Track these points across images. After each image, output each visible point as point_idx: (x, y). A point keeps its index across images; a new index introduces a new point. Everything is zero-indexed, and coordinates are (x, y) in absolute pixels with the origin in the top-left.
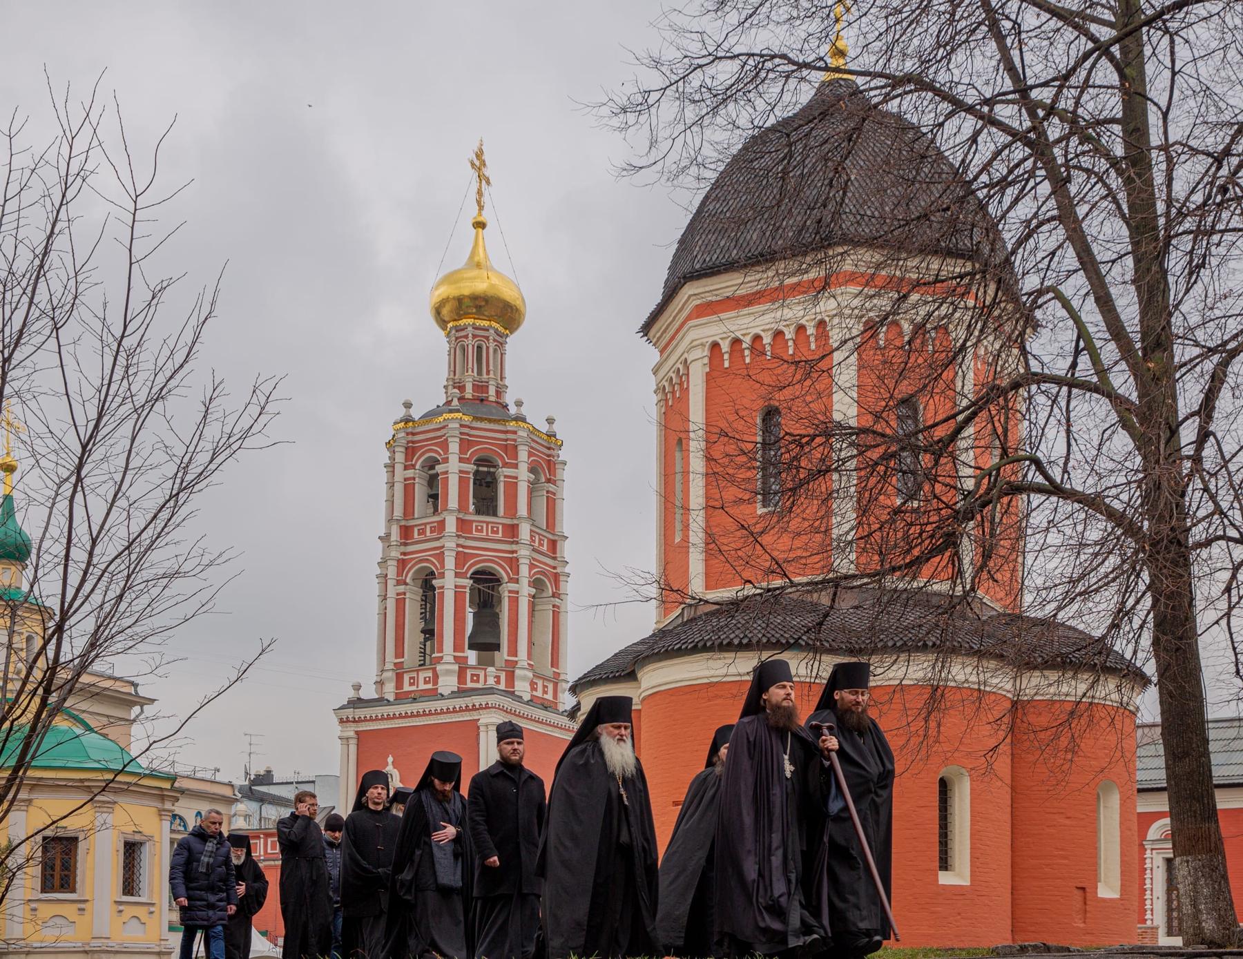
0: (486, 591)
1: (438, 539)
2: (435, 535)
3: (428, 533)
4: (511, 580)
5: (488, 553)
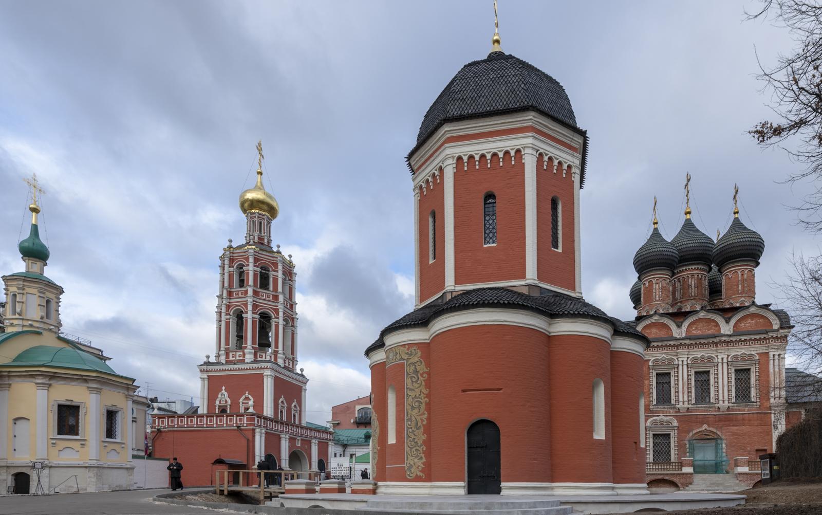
0: (264, 321)
1: (245, 297)
2: (243, 296)
3: (240, 295)
4: (276, 318)
5: (266, 305)
